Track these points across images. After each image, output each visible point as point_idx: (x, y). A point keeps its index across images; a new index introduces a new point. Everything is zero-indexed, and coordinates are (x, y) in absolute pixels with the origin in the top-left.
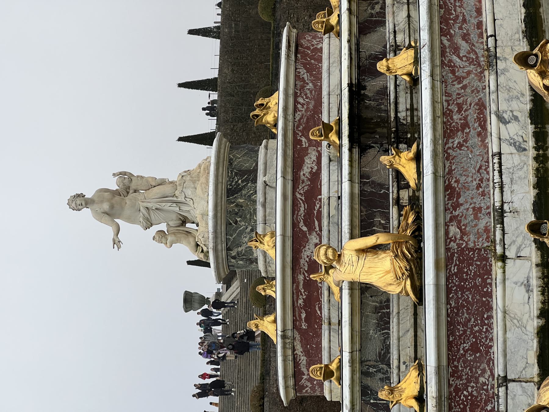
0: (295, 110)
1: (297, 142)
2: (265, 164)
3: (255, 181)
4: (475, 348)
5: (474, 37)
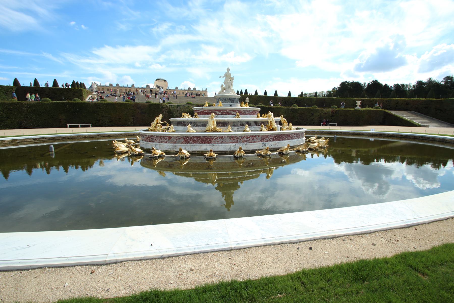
1: (237, 110)
4: (195, 141)
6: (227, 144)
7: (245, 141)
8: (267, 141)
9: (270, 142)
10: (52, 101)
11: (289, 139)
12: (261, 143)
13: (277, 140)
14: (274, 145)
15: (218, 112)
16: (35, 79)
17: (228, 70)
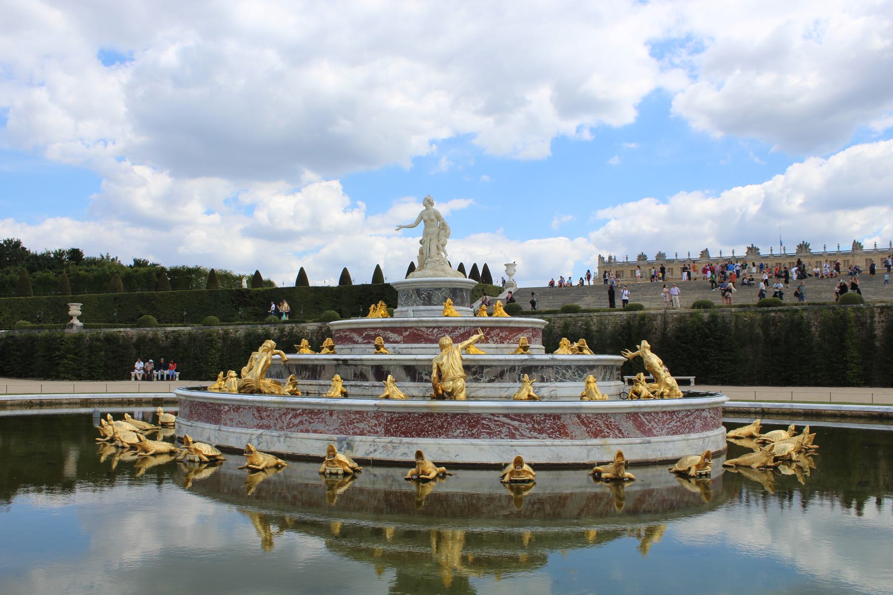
1: (406, 329)
2: (432, 310)
3: (424, 304)
5: (301, 427)
6: (244, 430)
8: (362, 433)
9: (370, 438)
11: (472, 436)
12: (335, 437)
13: (405, 434)
15: (356, 337)
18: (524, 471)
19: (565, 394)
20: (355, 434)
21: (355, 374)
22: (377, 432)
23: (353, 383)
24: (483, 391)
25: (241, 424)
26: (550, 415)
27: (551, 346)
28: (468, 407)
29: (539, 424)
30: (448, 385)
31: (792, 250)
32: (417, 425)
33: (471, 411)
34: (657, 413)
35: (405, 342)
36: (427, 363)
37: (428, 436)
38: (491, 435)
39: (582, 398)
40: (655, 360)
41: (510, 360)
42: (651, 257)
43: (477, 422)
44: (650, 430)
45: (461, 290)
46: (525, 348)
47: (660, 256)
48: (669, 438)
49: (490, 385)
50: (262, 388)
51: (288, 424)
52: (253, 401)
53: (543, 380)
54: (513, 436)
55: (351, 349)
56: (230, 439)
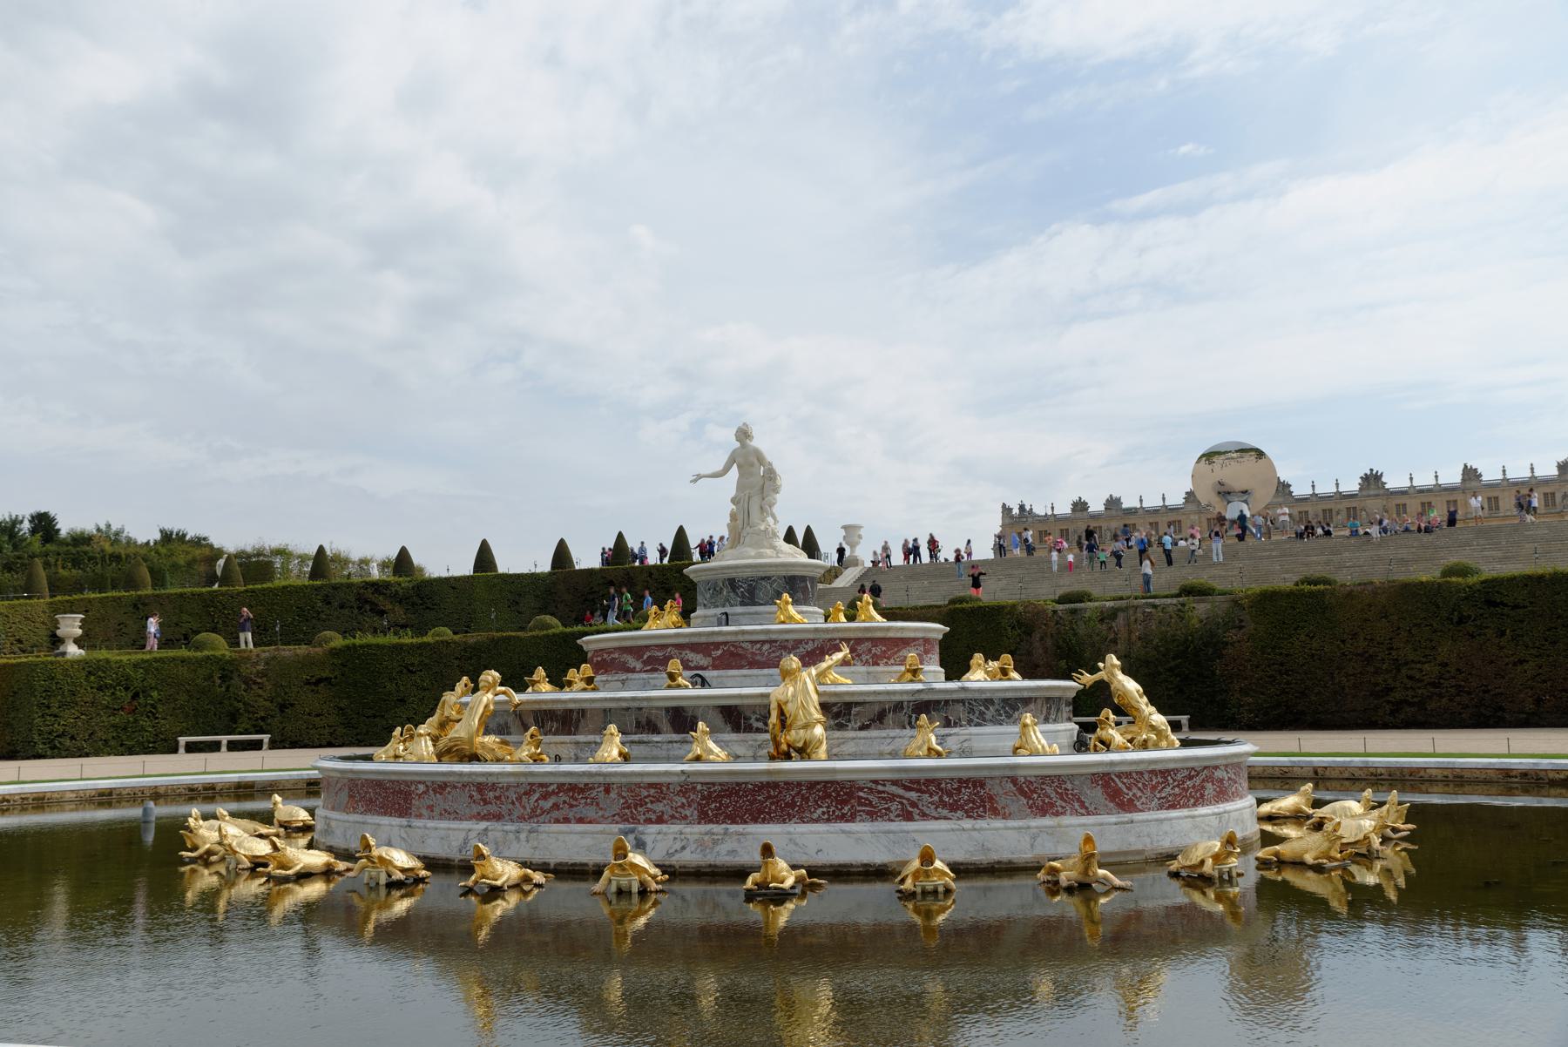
0: (753, 642)
1: (717, 645)
3: (743, 604)
5: (556, 814)
7: (534, 815)
8: (660, 820)
9: (675, 828)
10: (565, 626)
11: (843, 818)
14: (701, 844)
15: (632, 662)
16: (620, 536)
17: (743, 434)
18: (936, 870)
19: (987, 749)
20: (649, 821)
21: (638, 723)
22: (685, 817)
23: (636, 737)
24: (852, 743)
25: (448, 814)
26: (967, 781)
27: (955, 667)
28: (834, 771)
29: (950, 795)
30: (795, 736)
31: (1351, 485)
32: (752, 803)
33: (839, 777)
34: (1141, 773)
35: (715, 667)
36: (758, 701)
37: (770, 820)
38: (873, 815)
39: (1015, 751)
40: (1131, 686)
41: (894, 693)
42: (1096, 505)
43: (850, 795)
44: (1131, 801)
45: (803, 579)
46: (915, 672)
47: (1113, 503)
48: (1163, 814)
49: (863, 734)
50: (480, 752)
51: (533, 810)
52: (470, 774)
53: (947, 723)
54: (908, 817)
55: (623, 682)
56: (430, 841)
